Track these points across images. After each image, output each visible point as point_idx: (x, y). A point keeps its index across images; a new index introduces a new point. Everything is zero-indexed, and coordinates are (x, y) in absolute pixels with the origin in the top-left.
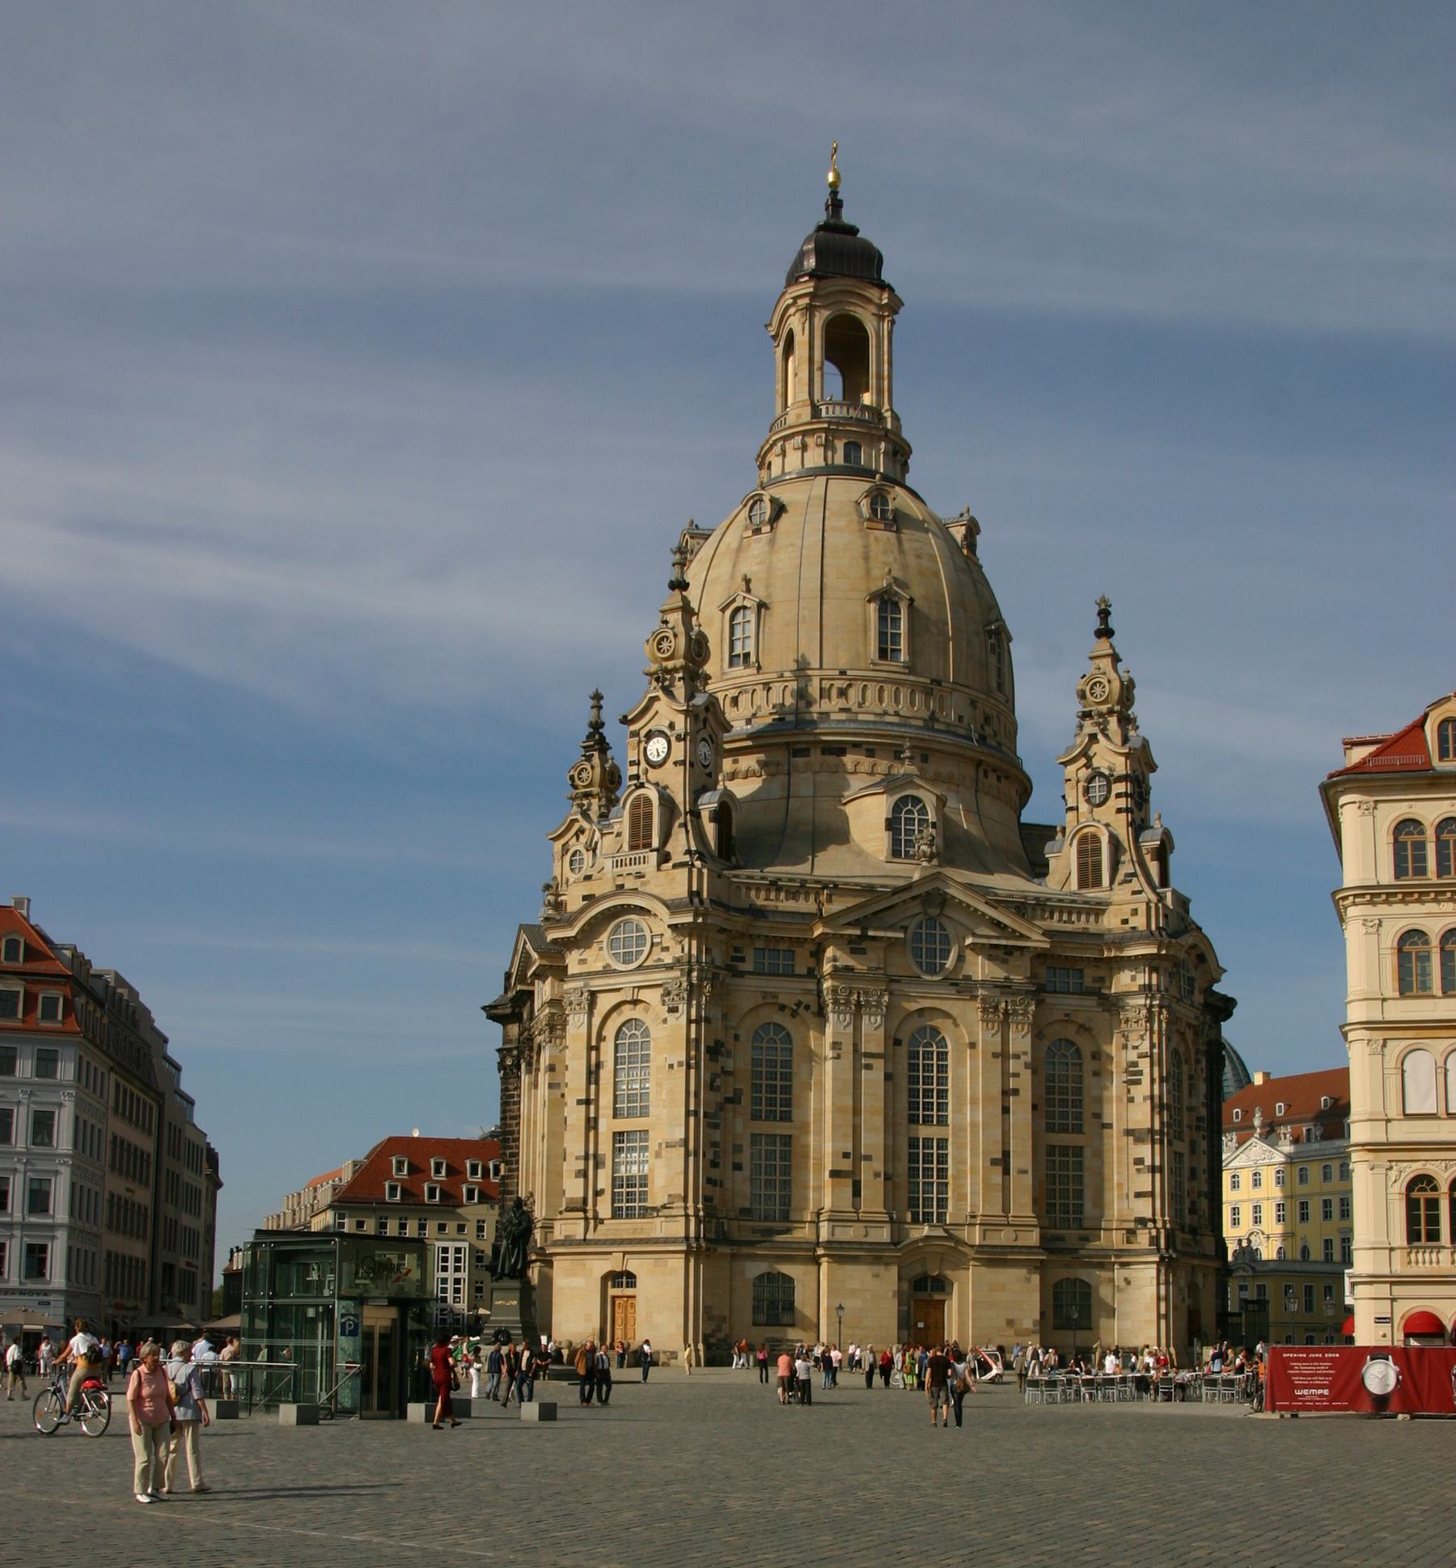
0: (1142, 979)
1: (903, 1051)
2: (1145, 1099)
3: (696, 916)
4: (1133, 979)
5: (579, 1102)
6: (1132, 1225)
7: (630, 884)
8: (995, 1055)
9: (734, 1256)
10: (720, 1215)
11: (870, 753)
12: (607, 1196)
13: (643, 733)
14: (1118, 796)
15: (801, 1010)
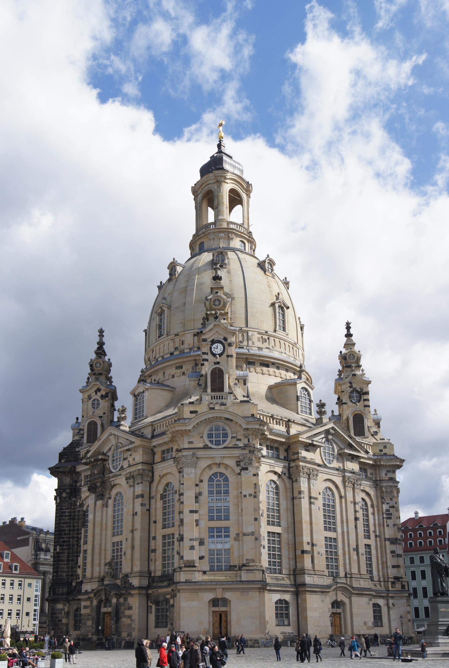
0: (390, 475)
1: (320, 497)
2: (394, 525)
3: (260, 425)
4: (386, 474)
5: (191, 512)
6: (392, 580)
7: (217, 407)
8: (351, 502)
9: (270, 590)
10: (265, 569)
11: (278, 368)
12: (206, 560)
13: (209, 340)
14: (365, 400)
15: (283, 475)
